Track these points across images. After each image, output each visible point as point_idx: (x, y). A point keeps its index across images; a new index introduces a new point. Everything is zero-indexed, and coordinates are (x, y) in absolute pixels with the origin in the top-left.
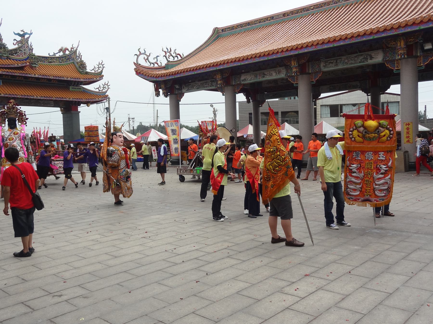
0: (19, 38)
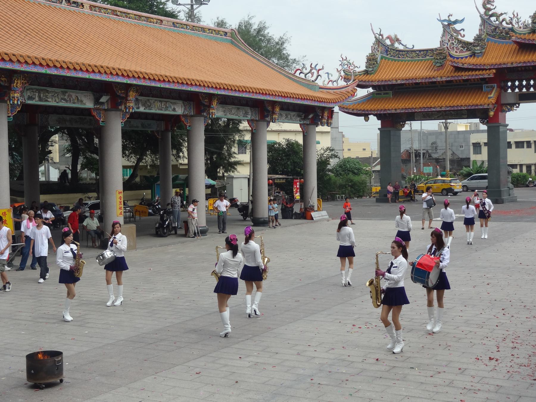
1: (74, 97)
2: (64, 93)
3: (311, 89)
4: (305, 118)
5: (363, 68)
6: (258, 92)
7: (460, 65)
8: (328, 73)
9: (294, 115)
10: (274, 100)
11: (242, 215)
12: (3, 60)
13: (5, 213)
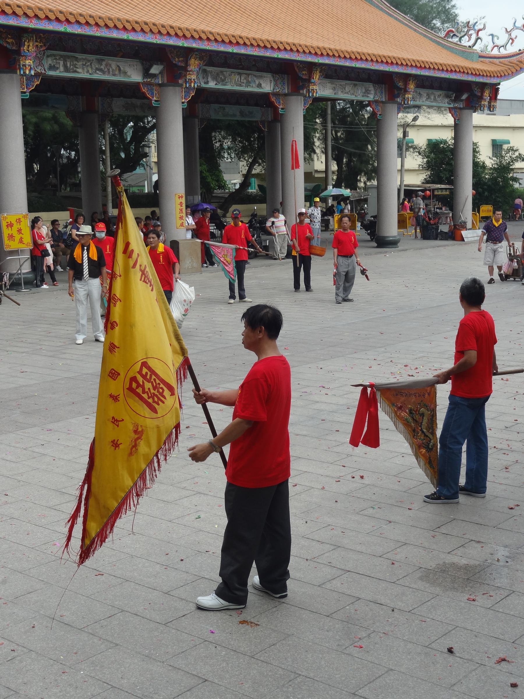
1: (114, 67)
2: (100, 61)
3: (467, 59)
4: (457, 99)
6: (380, 60)
8: (492, 35)
9: (439, 96)
10: (405, 71)
11: (368, 234)
12: (4, 12)
13: (19, 219)
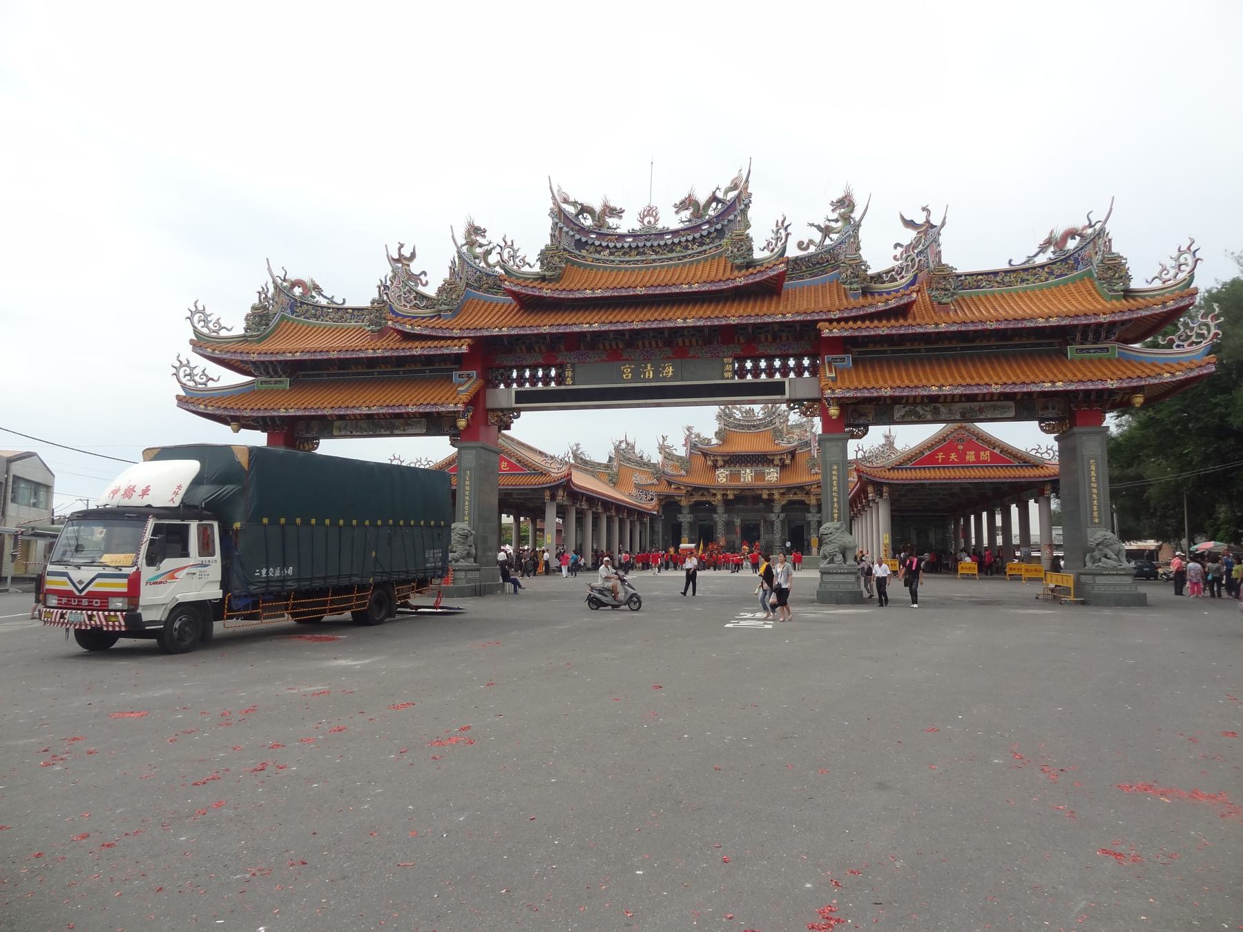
0: (909, 236)
5: (239, 330)
7: (408, 328)
